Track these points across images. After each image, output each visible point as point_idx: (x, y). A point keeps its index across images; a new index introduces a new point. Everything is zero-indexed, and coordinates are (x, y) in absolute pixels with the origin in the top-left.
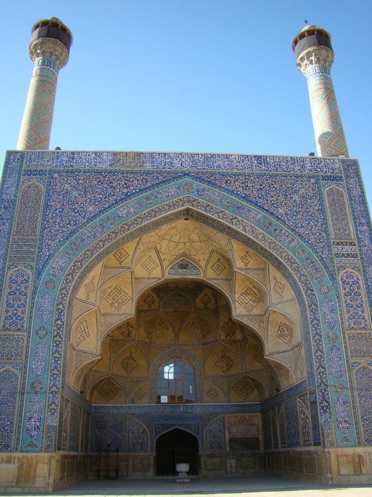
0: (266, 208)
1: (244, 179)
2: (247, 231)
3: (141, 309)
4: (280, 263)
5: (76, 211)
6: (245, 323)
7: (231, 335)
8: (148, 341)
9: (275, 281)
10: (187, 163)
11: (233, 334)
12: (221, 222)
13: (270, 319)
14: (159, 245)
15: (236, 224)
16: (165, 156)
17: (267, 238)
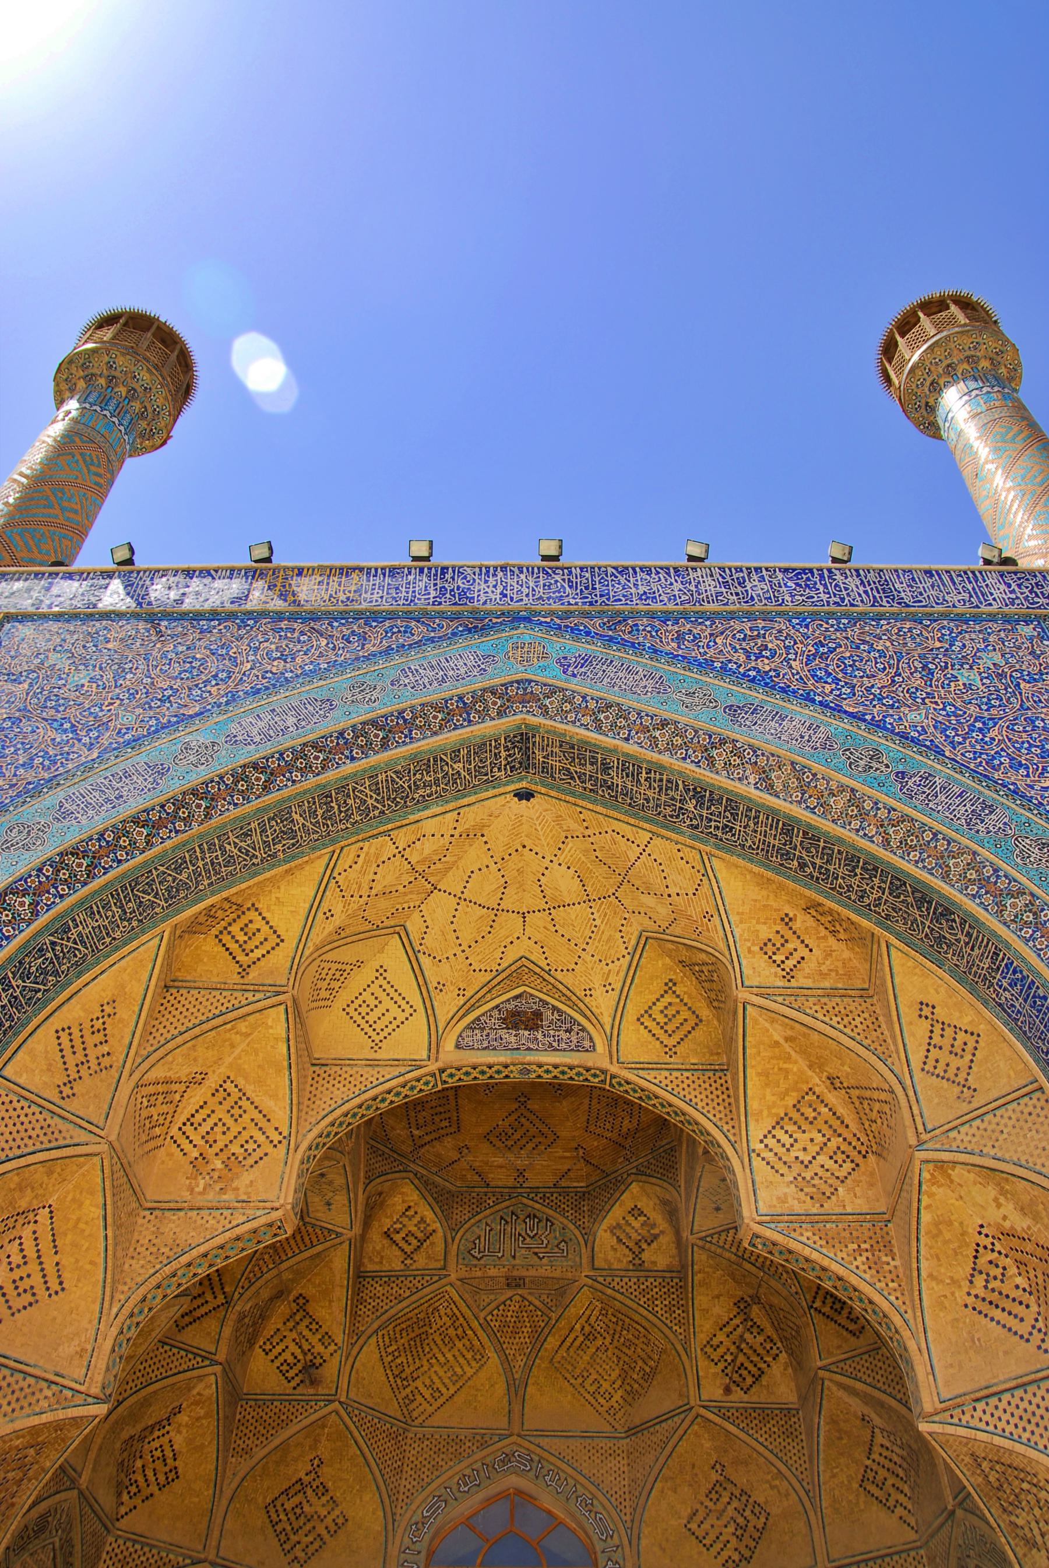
0: (851, 710)
1: (751, 629)
2: (778, 785)
3: (370, 1267)
4: (946, 912)
5: (67, 726)
6: (807, 1252)
7: (749, 1380)
8: (393, 1409)
9: (926, 1025)
10: (525, 591)
11: (757, 1379)
12: (661, 768)
13: (926, 1217)
14: (416, 915)
15: (727, 765)
16: (443, 573)
17: (868, 805)
